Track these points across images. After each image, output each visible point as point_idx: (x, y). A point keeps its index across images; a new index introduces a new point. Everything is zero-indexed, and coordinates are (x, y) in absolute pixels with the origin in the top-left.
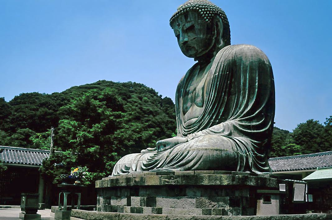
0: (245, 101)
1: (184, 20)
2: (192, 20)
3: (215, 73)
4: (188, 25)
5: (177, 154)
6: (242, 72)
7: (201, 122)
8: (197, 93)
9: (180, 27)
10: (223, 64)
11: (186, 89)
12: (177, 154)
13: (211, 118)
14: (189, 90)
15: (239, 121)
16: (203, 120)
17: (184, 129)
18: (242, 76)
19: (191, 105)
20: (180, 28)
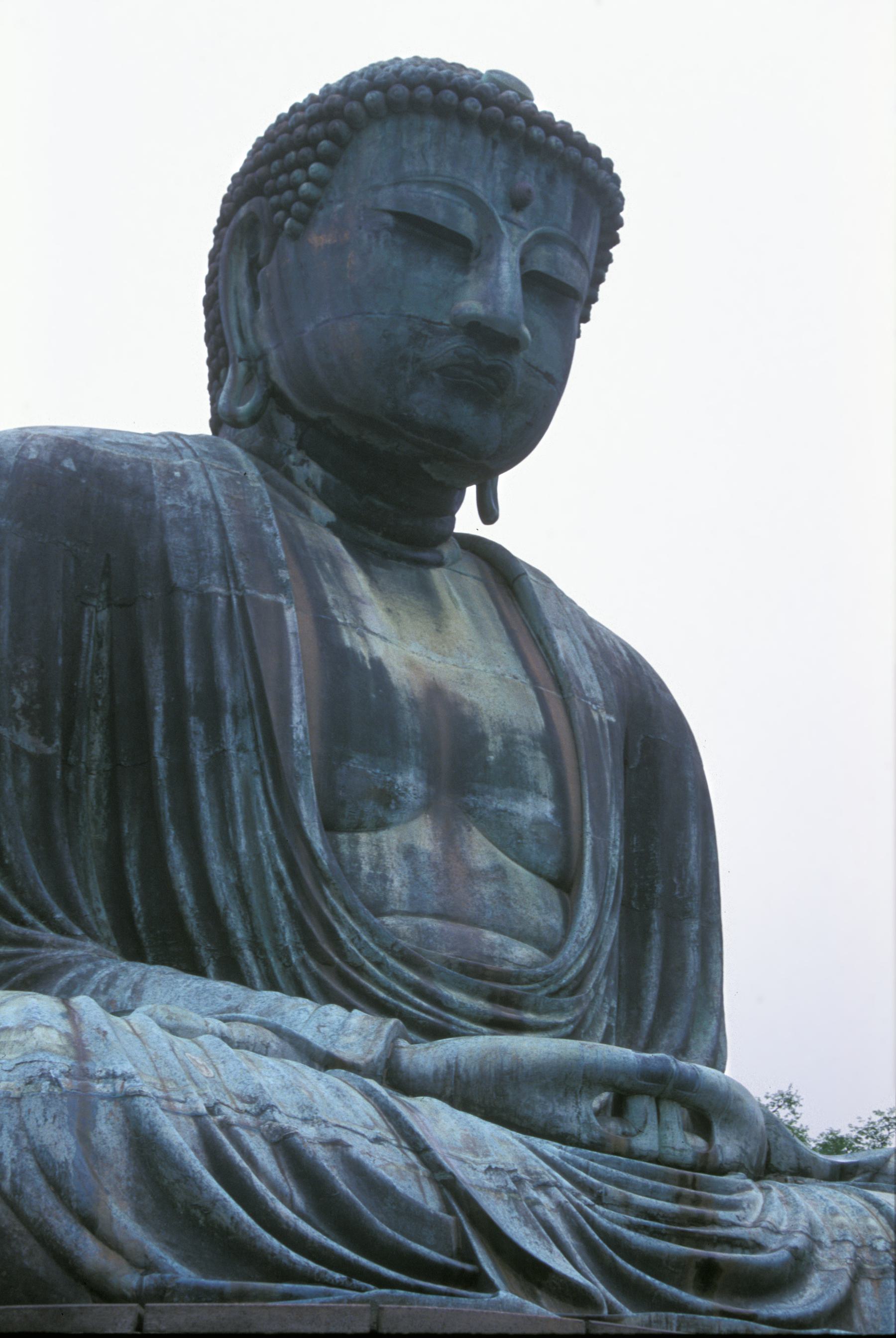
1: (569, 215)
8: (495, 745)
9: (520, 218)
14: (378, 666)
18: (694, 831)
20: (520, 226)
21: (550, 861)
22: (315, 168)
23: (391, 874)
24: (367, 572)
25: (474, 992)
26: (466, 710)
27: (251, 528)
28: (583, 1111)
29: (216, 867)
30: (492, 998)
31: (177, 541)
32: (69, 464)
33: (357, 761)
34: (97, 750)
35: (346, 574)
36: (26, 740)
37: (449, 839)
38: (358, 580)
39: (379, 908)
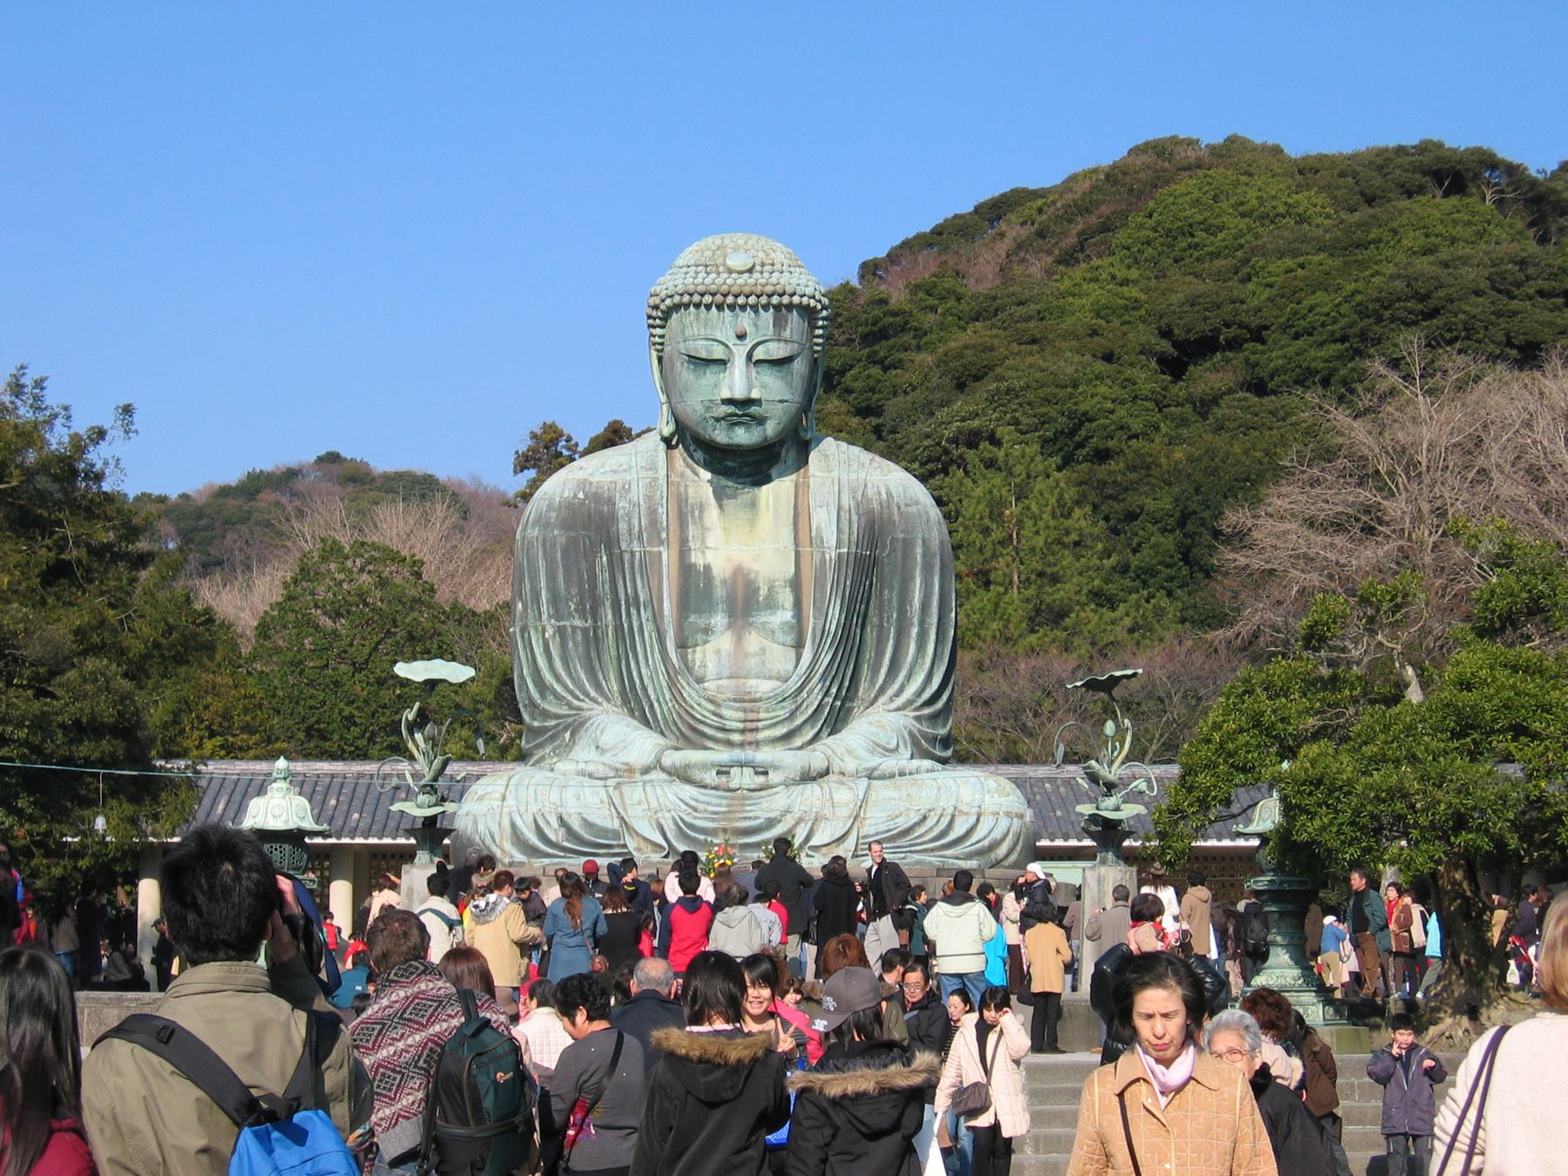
0: (928, 661)
2: (795, 338)
3: (838, 546)
4: (777, 350)
5: (925, 818)
6: (918, 568)
7: (799, 700)
8: (763, 592)
10: (855, 518)
11: (684, 552)
12: (925, 818)
13: (826, 694)
14: (708, 568)
15: (918, 718)
16: (804, 694)
17: (712, 707)
19: (730, 626)
21: (790, 639)
22: (658, 331)
23: (710, 665)
24: (721, 506)
25: (738, 710)
26: (752, 576)
27: (653, 512)
28: (710, 777)
29: (643, 670)
30: (745, 711)
31: (623, 526)
32: (581, 495)
33: (692, 618)
34: (610, 617)
35: (706, 514)
36: (578, 622)
37: (739, 641)
38: (713, 512)
39: (700, 680)
